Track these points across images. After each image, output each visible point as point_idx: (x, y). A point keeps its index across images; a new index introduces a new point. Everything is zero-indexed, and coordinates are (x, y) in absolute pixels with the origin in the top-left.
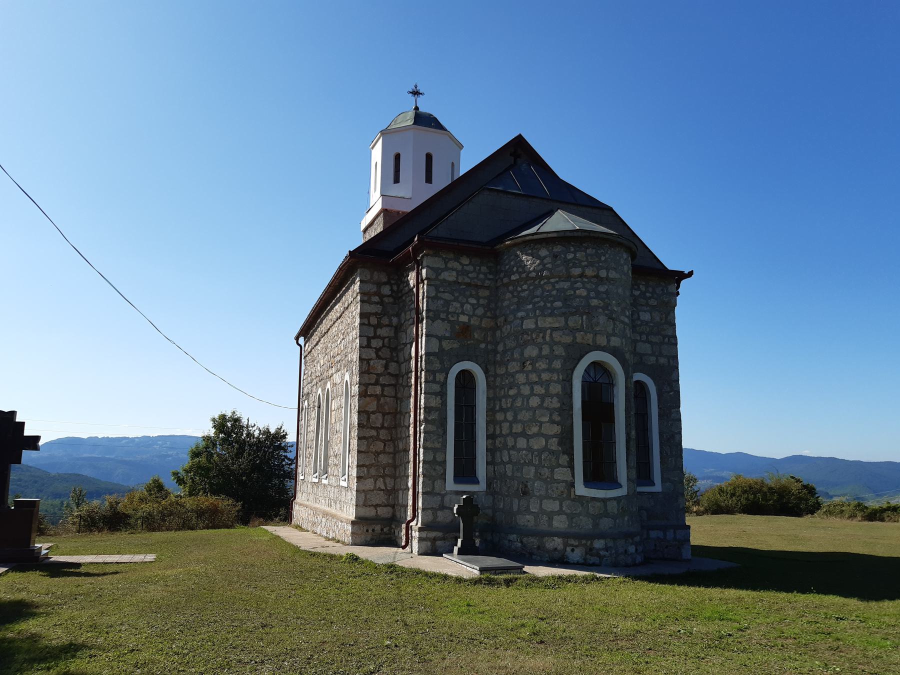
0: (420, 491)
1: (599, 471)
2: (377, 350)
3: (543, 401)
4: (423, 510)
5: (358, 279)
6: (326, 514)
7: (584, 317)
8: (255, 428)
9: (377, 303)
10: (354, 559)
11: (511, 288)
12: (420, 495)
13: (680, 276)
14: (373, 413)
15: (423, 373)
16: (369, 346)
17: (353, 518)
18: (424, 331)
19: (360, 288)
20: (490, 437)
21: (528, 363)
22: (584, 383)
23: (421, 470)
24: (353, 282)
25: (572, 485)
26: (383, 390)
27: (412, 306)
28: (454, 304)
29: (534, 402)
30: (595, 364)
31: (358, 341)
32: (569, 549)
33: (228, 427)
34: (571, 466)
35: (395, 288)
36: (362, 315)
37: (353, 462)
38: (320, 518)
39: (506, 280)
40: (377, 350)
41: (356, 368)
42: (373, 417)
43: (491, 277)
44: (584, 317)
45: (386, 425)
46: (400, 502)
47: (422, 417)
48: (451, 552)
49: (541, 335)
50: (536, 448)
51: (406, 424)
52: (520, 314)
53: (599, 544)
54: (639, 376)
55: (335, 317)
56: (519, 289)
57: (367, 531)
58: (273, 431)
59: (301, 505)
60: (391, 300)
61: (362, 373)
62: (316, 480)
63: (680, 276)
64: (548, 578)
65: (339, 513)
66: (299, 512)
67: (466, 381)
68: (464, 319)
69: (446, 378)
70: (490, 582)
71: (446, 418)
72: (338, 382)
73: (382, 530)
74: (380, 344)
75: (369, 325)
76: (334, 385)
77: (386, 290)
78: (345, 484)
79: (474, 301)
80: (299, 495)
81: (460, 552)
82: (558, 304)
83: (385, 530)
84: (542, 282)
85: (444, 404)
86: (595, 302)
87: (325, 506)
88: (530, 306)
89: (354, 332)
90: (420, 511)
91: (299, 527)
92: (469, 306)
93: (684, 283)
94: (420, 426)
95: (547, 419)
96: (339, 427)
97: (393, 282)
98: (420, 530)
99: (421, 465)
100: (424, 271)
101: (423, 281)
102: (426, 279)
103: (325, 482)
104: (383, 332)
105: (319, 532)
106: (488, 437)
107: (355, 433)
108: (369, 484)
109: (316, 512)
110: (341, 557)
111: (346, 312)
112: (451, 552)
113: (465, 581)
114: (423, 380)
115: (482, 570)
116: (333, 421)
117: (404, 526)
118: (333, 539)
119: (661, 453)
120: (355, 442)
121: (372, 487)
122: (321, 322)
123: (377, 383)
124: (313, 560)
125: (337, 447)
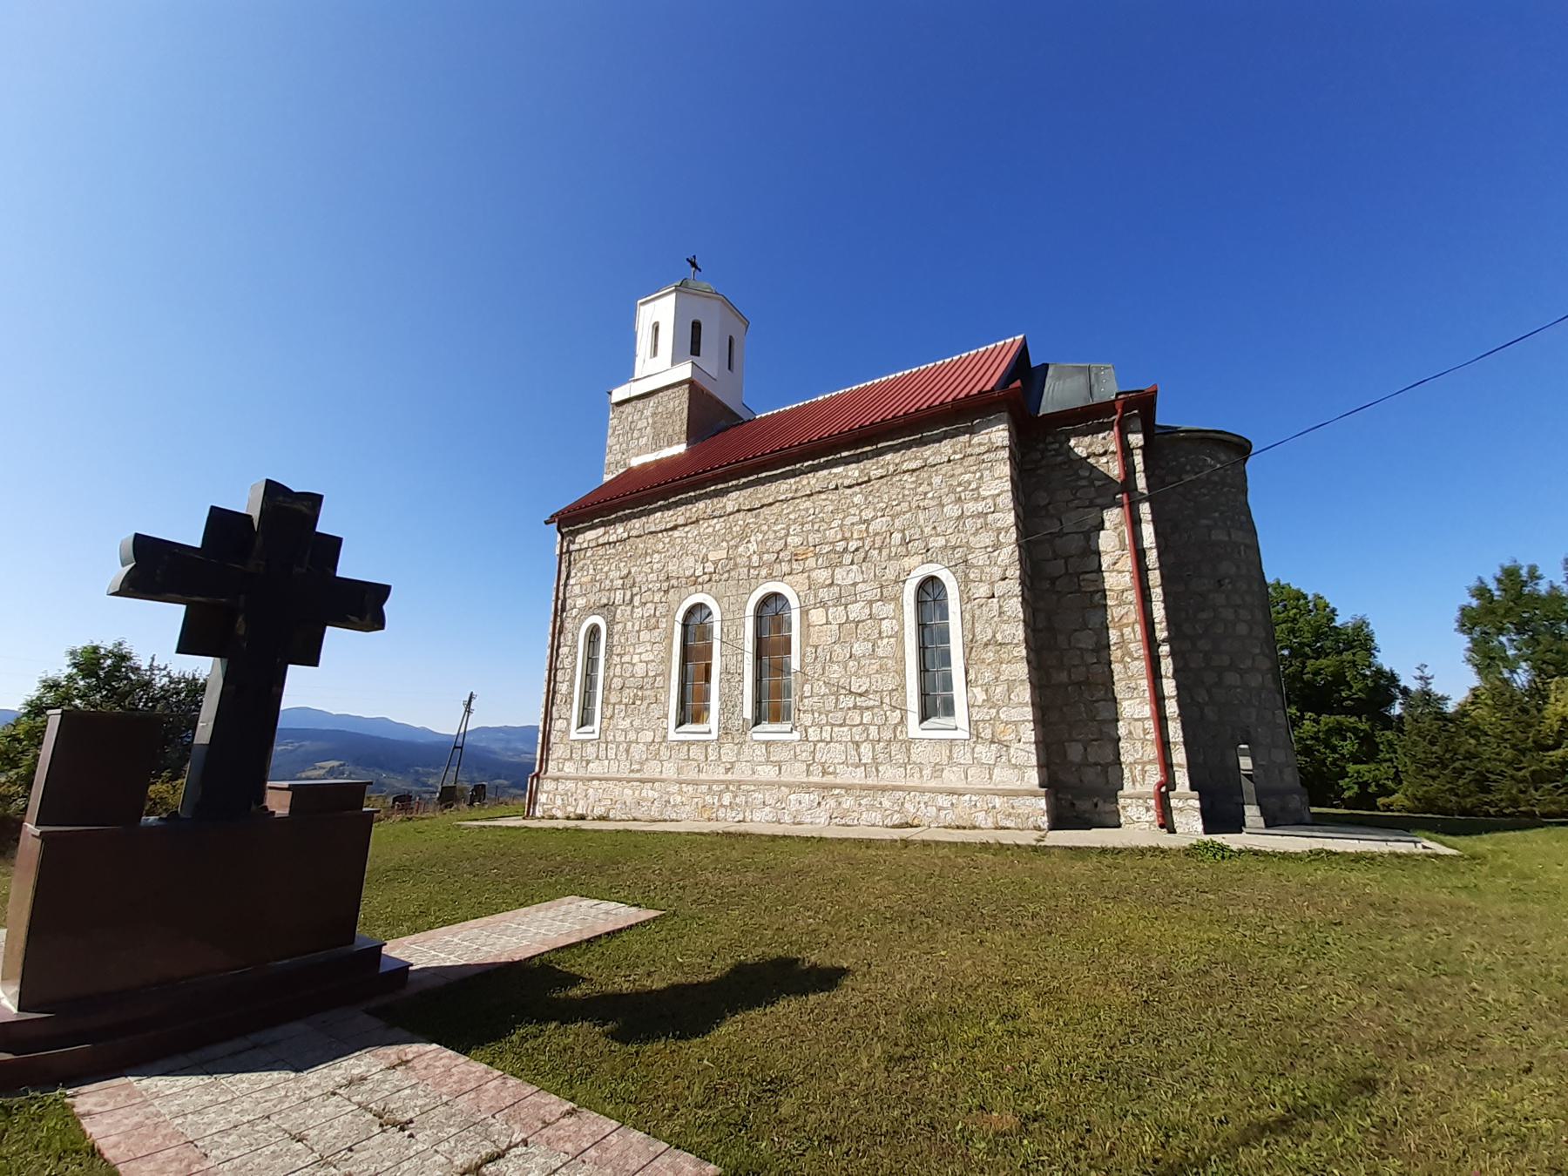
3: (1251, 629)
29: (1242, 629)
52: (1204, 522)
100: (1136, 439)
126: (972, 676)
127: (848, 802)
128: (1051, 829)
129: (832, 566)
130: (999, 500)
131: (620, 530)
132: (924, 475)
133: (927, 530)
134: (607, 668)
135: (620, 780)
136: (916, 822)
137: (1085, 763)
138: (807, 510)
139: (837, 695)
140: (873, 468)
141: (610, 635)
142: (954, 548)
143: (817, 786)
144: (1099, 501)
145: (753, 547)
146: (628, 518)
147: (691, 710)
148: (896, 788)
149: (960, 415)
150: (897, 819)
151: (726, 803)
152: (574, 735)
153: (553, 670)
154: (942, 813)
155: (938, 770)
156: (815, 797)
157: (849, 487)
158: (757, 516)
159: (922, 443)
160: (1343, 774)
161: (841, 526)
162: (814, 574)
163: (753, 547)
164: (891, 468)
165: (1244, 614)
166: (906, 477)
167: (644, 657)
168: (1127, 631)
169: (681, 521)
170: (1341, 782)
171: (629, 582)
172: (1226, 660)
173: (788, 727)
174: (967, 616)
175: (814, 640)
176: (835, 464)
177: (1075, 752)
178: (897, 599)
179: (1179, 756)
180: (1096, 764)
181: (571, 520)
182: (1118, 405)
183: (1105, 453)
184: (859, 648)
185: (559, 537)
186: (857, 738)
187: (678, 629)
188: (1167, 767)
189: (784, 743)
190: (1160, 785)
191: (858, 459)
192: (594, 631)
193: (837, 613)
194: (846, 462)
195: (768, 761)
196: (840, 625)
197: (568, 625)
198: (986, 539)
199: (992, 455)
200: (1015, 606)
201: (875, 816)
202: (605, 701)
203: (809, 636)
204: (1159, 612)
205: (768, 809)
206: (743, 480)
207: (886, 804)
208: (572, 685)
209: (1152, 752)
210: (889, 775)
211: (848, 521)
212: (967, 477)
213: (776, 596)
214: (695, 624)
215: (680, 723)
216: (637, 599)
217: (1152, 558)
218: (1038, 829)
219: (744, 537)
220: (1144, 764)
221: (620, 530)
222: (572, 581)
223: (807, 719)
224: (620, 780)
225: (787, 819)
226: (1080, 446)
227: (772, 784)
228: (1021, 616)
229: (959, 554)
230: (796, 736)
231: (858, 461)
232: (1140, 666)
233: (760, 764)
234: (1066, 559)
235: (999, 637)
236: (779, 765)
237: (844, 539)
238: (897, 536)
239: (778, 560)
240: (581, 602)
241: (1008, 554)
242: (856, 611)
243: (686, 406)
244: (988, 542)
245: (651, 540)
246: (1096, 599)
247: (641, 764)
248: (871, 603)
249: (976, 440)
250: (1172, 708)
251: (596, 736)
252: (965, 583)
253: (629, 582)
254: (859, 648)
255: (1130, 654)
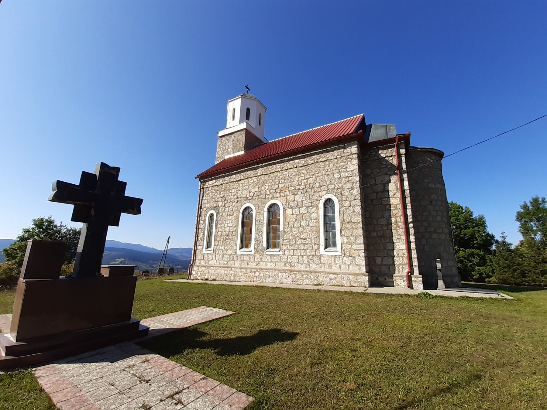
29: (439, 218)
52: (426, 181)
100: (403, 151)
126: (343, 233)
127: (299, 276)
128: (370, 287)
129: (294, 194)
130: (353, 172)
131: (221, 181)
132: (327, 163)
133: (328, 182)
134: (216, 229)
135: (220, 267)
136: (322, 284)
137: (382, 264)
138: (286, 175)
139: (295, 239)
140: (309, 160)
141: (217, 217)
142: (337, 189)
143: (288, 270)
144: (389, 173)
145: (267, 187)
146: (224, 177)
147: (245, 244)
148: (315, 272)
149: (341, 142)
150: (316, 282)
151: (257, 276)
152: (204, 251)
153: (197, 229)
154: (332, 281)
155: (330, 266)
156: (287, 274)
157: (301, 167)
158: (269, 177)
159: (327, 152)
160: (474, 270)
161: (298, 181)
162: (288, 197)
163: (267, 187)
164: (316, 161)
165: (440, 213)
166: (321, 163)
167: (229, 225)
168: (398, 218)
169: (242, 178)
170: (473, 273)
171: (224, 199)
172: (433, 230)
173: (278, 250)
174: (342, 213)
175: (288, 220)
176: (296, 159)
177: (379, 261)
178: (317, 206)
179: (415, 263)
180: (386, 265)
181: (204, 177)
182: (397, 139)
183: (391, 156)
184: (304, 223)
185: (200, 183)
186: (302, 254)
187: (241, 215)
188: (411, 266)
189: (277, 255)
190: (408, 273)
191: (304, 157)
192: (212, 216)
193: (296, 211)
194: (300, 158)
195: (271, 262)
196: (297, 215)
197: (203, 213)
198: (349, 186)
199: (351, 156)
200: (358, 209)
201: (308, 281)
202: (215, 240)
203: (286, 219)
204: (409, 212)
205: (271, 278)
206: (264, 164)
207: (312, 277)
208: (204, 234)
209: (406, 261)
210: (313, 267)
211: (300, 179)
212: (342, 164)
213: (275, 204)
214: (247, 214)
215: (241, 248)
216: (227, 205)
217: (407, 193)
218: (365, 287)
219: (264, 184)
220: (403, 265)
221: (221, 181)
222: (204, 198)
223: (285, 247)
224: (220, 267)
225: (278, 282)
226: (383, 153)
227: (273, 269)
228: (361, 213)
229: (339, 191)
230: (281, 253)
231: (304, 158)
232: (402, 231)
233: (269, 263)
234: (377, 193)
235: (353, 220)
236: (275, 263)
237: (299, 185)
238: (317, 184)
239: (276, 192)
240: (207, 206)
241: (357, 191)
242: (303, 210)
243: (244, 138)
244: (349, 187)
245: (232, 184)
246: (387, 207)
247: (228, 262)
248: (308, 207)
249: (346, 151)
250: (413, 246)
251: (212, 252)
252: (341, 201)
253: (224, 199)
254: (304, 223)
255: (399, 227)
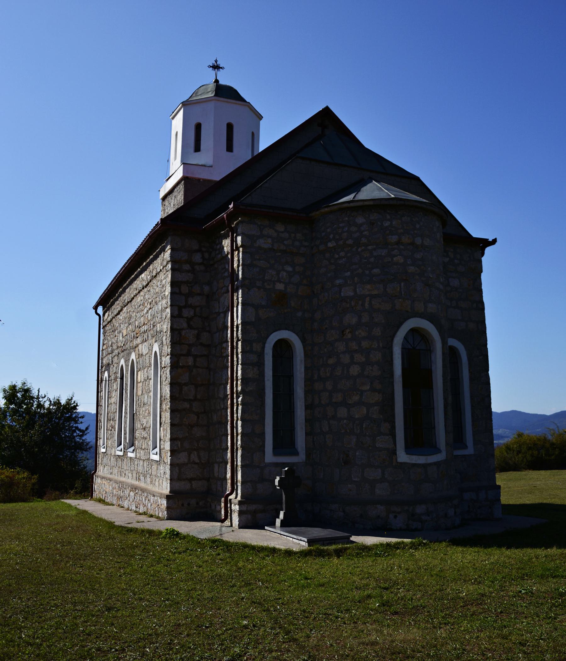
0: (239, 464)
1: (419, 439)
2: (189, 320)
4: (242, 483)
5: (169, 247)
6: (134, 488)
7: (402, 284)
8: (45, 399)
9: (188, 271)
10: (174, 534)
11: (327, 255)
12: (239, 469)
13: (486, 243)
14: (186, 384)
15: (240, 343)
16: (180, 316)
17: (167, 491)
18: (240, 299)
19: (172, 256)
20: (308, 407)
21: (348, 331)
22: (403, 349)
23: (239, 443)
24: (163, 250)
25: (394, 452)
26: (195, 361)
27: (226, 274)
28: (270, 271)
29: (355, 370)
30: (414, 331)
31: (168, 310)
32: (391, 516)
33: (18, 398)
34: (393, 434)
35: (206, 255)
36: (173, 284)
37: (165, 435)
38: (127, 492)
39: (322, 247)
40: (189, 320)
41: (166, 339)
42: (185, 388)
43: (306, 244)
44: (402, 284)
45: (199, 397)
46: (216, 475)
47: (239, 388)
48: (273, 524)
49: (360, 303)
50: (357, 417)
51: (221, 396)
52: (338, 282)
53: (420, 509)
54: (452, 342)
55: (141, 286)
56: (337, 256)
57: (183, 505)
58: (63, 402)
59: (103, 478)
60: (202, 268)
61: (174, 343)
62: (121, 453)
63: (486, 243)
64: (376, 546)
65: (150, 487)
66: (100, 486)
67: (283, 350)
68: (280, 286)
69: (263, 348)
70: (321, 554)
71: (264, 389)
72: (144, 353)
73: (197, 503)
74: (192, 313)
75: (180, 293)
76: (140, 356)
77: (197, 258)
78: (157, 458)
79: (289, 269)
80: (100, 468)
81: (283, 524)
82: (376, 271)
83: (201, 503)
84: (360, 250)
85: (262, 374)
86: (412, 269)
87: (134, 480)
88: (348, 274)
89: (164, 302)
90: (239, 484)
91: (101, 501)
92: (285, 274)
93: (488, 250)
94: (238, 397)
95: (368, 387)
96: (148, 398)
97: (204, 249)
98: (240, 503)
99: (239, 437)
100: (239, 239)
101: (237, 249)
102: (241, 246)
103: (130, 455)
104: (195, 301)
105: (126, 506)
106: (307, 407)
107: (167, 406)
108: (183, 458)
109: (122, 486)
110: (161, 533)
111: (154, 281)
112: (273, 524)
113: (296, 553)
114: (240, 350)
115: (310, 542)
116: (140, 393)
117: (223, 499)
118: (145, 513)
119: (472, 416)
120: (167, 416)
121: (186, 461)
122: (124, 291)
123: (189, 354)
124: (132, 536)
125: (145, 419)
